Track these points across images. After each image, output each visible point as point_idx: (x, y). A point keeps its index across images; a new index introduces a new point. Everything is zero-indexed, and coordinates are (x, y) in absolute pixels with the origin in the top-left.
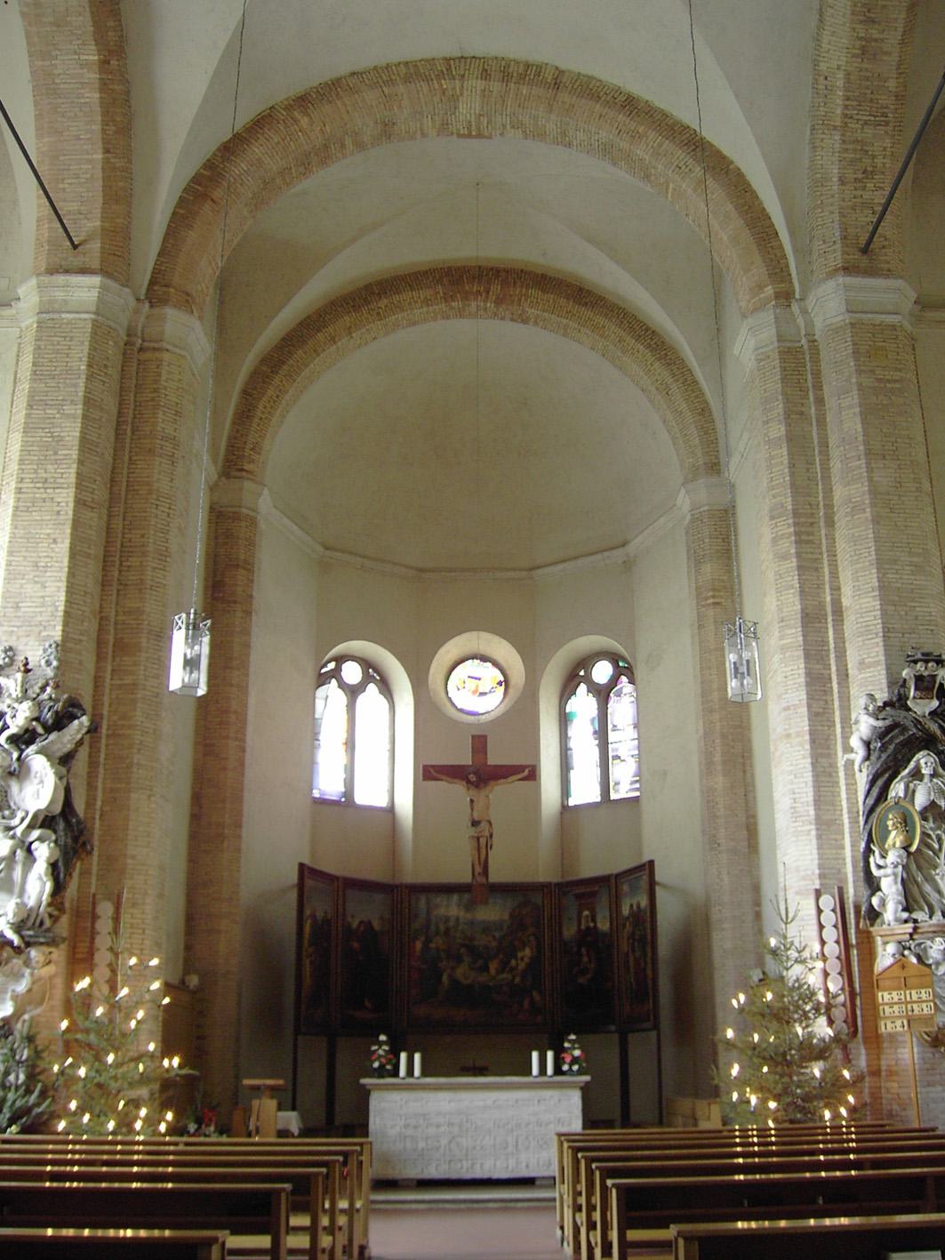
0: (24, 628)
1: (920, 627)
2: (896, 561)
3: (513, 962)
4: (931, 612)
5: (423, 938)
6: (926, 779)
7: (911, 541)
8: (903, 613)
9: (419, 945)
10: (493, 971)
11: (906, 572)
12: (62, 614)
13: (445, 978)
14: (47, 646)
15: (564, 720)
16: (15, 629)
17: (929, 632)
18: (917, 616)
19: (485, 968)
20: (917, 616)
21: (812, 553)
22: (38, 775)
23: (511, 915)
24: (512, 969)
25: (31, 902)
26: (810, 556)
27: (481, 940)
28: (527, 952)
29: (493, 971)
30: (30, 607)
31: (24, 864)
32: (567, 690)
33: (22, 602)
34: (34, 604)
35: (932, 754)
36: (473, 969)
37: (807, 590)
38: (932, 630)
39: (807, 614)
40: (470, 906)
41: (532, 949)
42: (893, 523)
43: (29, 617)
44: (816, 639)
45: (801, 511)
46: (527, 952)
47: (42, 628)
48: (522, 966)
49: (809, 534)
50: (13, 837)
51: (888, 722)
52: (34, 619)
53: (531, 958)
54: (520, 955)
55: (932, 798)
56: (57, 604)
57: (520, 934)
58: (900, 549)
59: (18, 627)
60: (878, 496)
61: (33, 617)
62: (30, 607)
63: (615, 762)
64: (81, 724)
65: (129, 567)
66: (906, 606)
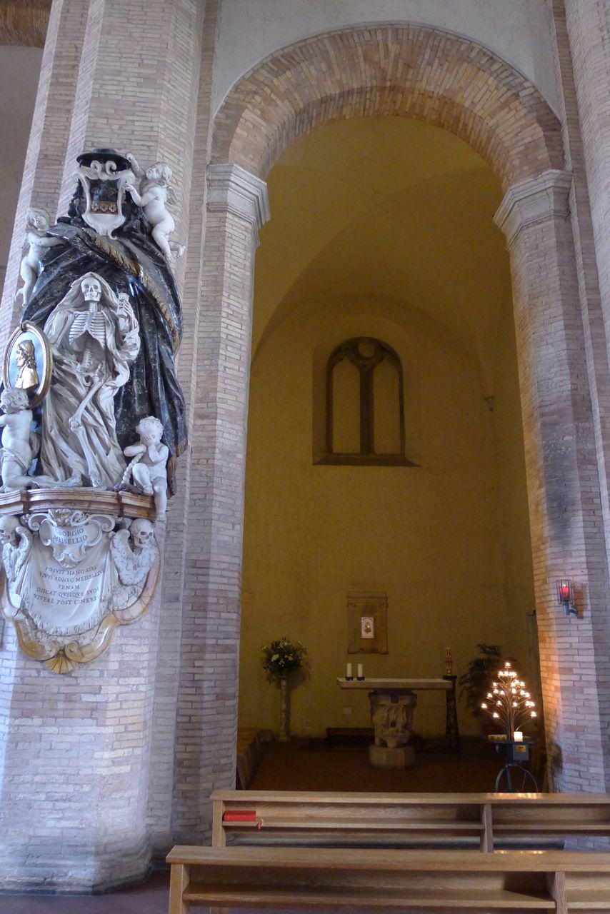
1: (134, 143)
2: (121, 72)
4: (152, 127)
6: (93, 307)
7: (144, 52)
8: (116, 127)
11: (131, 84)
17: (146, 148)
18: (133, 131)
20: (133, 131)
21: (67, 95)
26: (63, 98)
35: (97, 276)
37: (51, 131)
38: (149, 147)
39: (46, 156)
42: (128, 34)
44: (50, 181)
45: (64, 54)
49: (67, 76)
51: (53, 241)
55: (84, 330)
58: (129, 60)
60: (117, 6)
66: (123, 119)
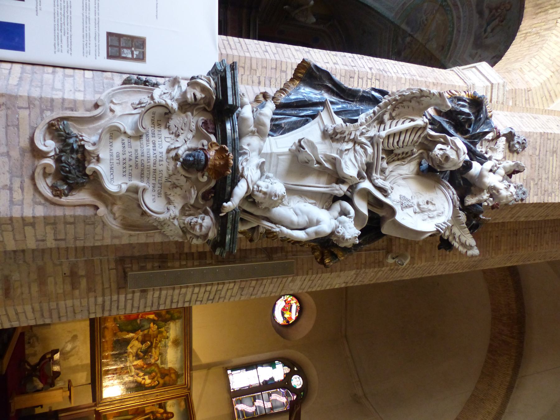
0: (537, 162)
3: (141, 374)
5: (156, 318)
9: (152, 316)
10: (135, 363)
12: (546, 201)
13: (131, 335)
14: (524, 189)
15: (271, 363)
16: (537, 152)
19: (137, 357)
22: (430, 207)
23: (170, 369)
24: (137, 374)
25: (280, 211)
27: (155, 353)
28: (148, 381)
29: (135, 363)
30: (553, 167)
31: (323, 194)
32: (286, 362)
33: (557, 157)
34: (554, 169)
36: (138, 350)
40: (176, 343)
41: (150, 383)
43: (546, 166)
46: (148, 381)
47: (536, 182)
48: (139, 379)
50: (360, 175)
52: (543, 172)
53: (144, 384)
54: (146, 377)
56: (553, 194)
57: (159, 375)
59: (539, 155)
61: (545, 169)
62: (553, 167)
63: (252, 398)
64: (471, 247)
65: (528, 235)
